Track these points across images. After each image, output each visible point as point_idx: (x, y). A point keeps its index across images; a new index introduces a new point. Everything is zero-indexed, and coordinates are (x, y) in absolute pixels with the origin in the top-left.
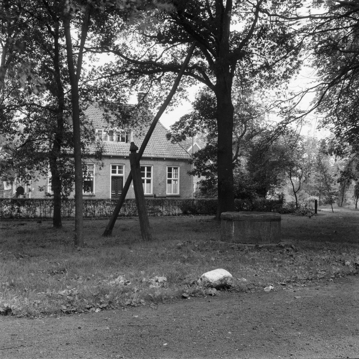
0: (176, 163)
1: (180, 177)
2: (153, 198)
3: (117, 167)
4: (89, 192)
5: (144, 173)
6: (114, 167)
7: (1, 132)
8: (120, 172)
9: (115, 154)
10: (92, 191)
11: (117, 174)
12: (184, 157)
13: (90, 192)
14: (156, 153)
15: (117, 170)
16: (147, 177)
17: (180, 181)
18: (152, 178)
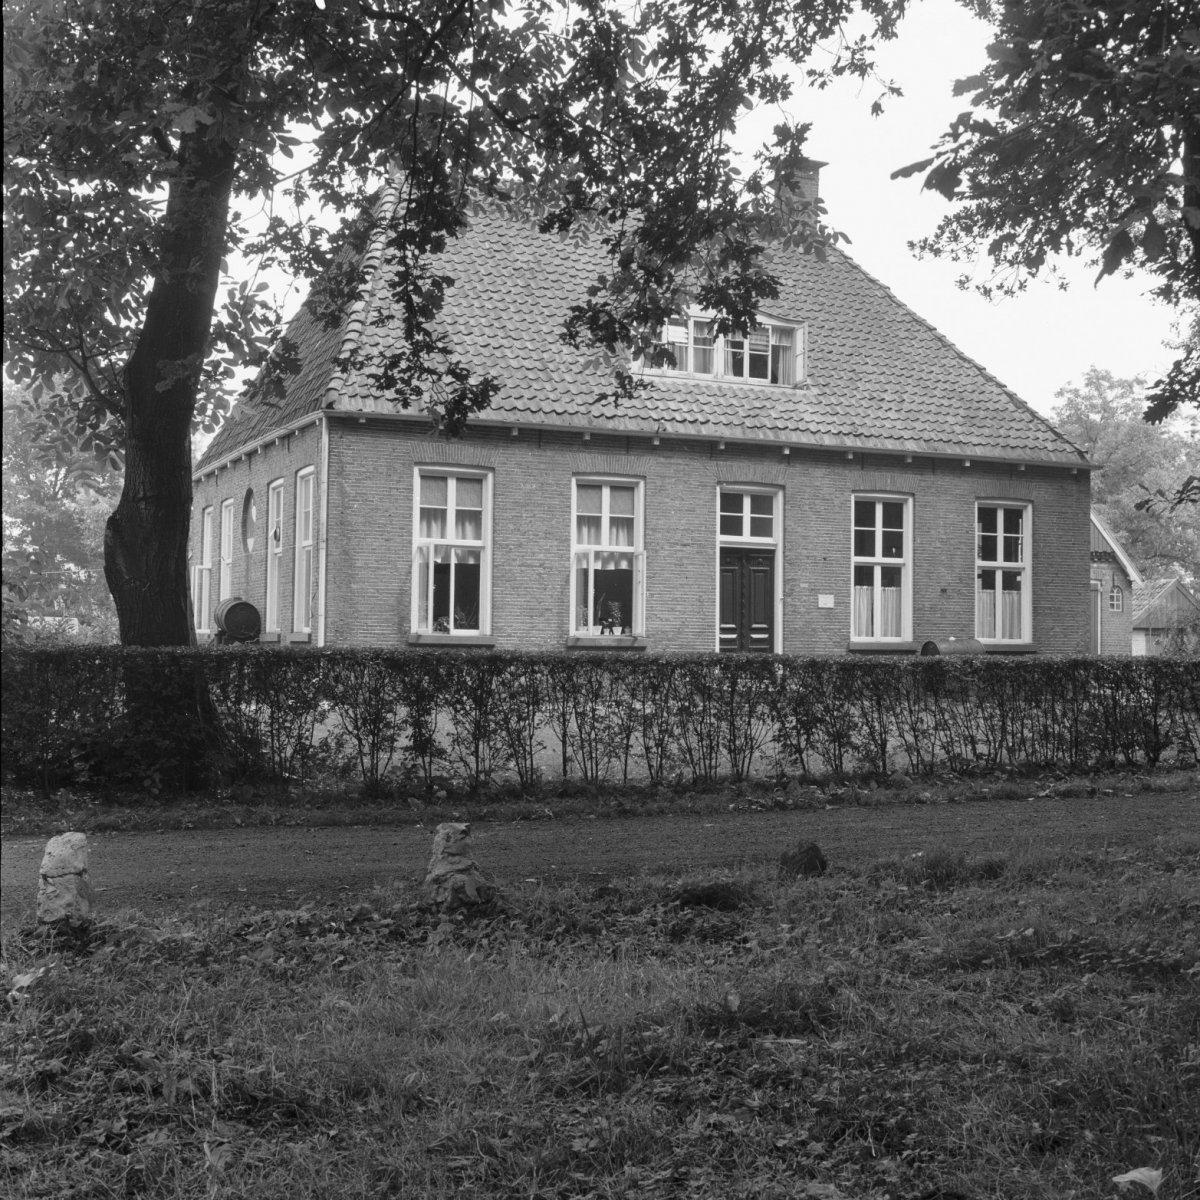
0: (1020, 488)
1: (1035, 556)
2: (919, 658)
3: (747, 503)
4: (611, 626)
5: (740, 519)
6: (731, 502)
7: (1196, 483)
8: (761, 528)
9: (737, 434)
10: (627, 622)
11: (746, 539)
12: (1053, 458)
13: (618, 630)
14: (926, 436)
15: (747, 515)
16: (887, 553)
17: (1035, 573)
18: (906, 561)
